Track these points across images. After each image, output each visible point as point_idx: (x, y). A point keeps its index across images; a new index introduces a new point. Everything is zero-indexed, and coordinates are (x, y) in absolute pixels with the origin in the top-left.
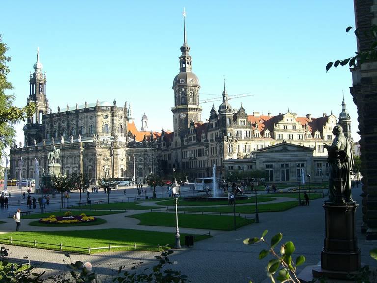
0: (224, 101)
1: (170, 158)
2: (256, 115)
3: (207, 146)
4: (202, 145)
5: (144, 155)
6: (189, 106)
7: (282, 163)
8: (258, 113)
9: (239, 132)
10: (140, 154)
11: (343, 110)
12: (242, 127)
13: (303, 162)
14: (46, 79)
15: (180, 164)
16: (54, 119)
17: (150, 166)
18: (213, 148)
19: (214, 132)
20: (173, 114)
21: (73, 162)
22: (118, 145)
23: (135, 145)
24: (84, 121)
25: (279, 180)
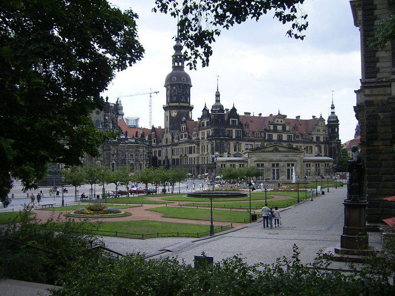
1: (160, 155)
2: (247, 115)
3: (198, 145)
4: (193, 142)
6: (181, 104)
11: (333, 113)
12: (234, 126)
15: (171, 160)
18: (204, 146)
19: (205, 131)
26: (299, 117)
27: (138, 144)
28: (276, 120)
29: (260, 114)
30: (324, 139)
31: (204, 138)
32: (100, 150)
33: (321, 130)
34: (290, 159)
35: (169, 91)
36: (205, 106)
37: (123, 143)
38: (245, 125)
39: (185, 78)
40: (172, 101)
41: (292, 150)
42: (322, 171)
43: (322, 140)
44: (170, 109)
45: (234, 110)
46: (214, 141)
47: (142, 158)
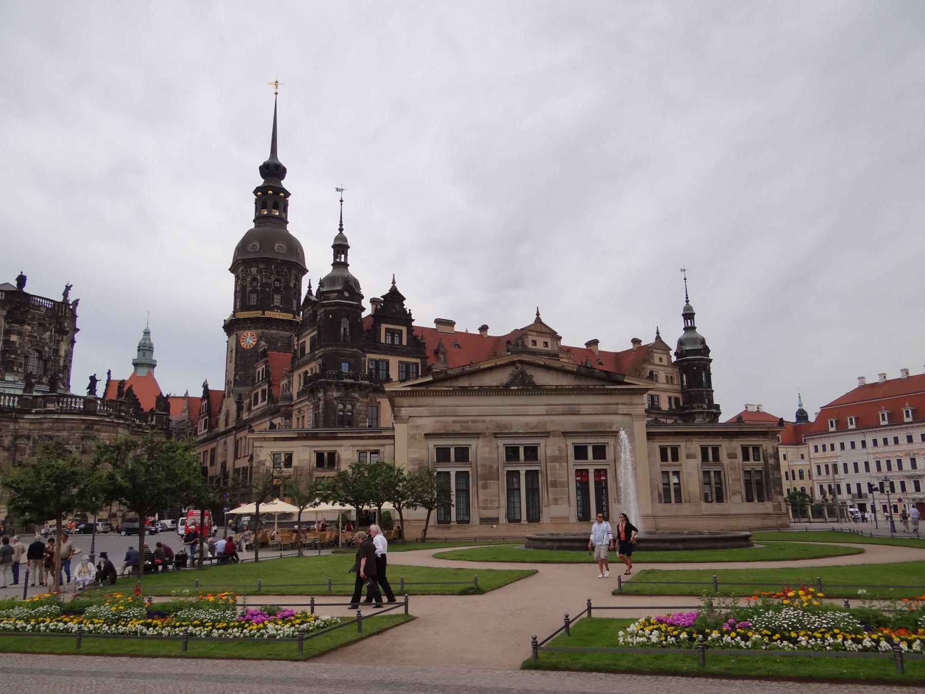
0: (336, 265)
2: (444, 329)
5: (83, 438)
6: (268, 314)
7: (510, 442)
8: (451, 324)
9: (382, 366)
10: (65, 434)
11: (690, 329)
12: (392, 350)
13: (600, 441)
23: (51, 407)
25: (495, 520)
26: (595, 342)
28: (530, 338)
29: (484, 328)
30: (670, 403)
33: (662, 377)
34: (583, 425)
37: (37, 413)
38: (436, 352)
41: (591, 383)
42: (734, 482)
43: (664, 406)
44: (239, 329)
45: (394, 297)
46: (321, 395)
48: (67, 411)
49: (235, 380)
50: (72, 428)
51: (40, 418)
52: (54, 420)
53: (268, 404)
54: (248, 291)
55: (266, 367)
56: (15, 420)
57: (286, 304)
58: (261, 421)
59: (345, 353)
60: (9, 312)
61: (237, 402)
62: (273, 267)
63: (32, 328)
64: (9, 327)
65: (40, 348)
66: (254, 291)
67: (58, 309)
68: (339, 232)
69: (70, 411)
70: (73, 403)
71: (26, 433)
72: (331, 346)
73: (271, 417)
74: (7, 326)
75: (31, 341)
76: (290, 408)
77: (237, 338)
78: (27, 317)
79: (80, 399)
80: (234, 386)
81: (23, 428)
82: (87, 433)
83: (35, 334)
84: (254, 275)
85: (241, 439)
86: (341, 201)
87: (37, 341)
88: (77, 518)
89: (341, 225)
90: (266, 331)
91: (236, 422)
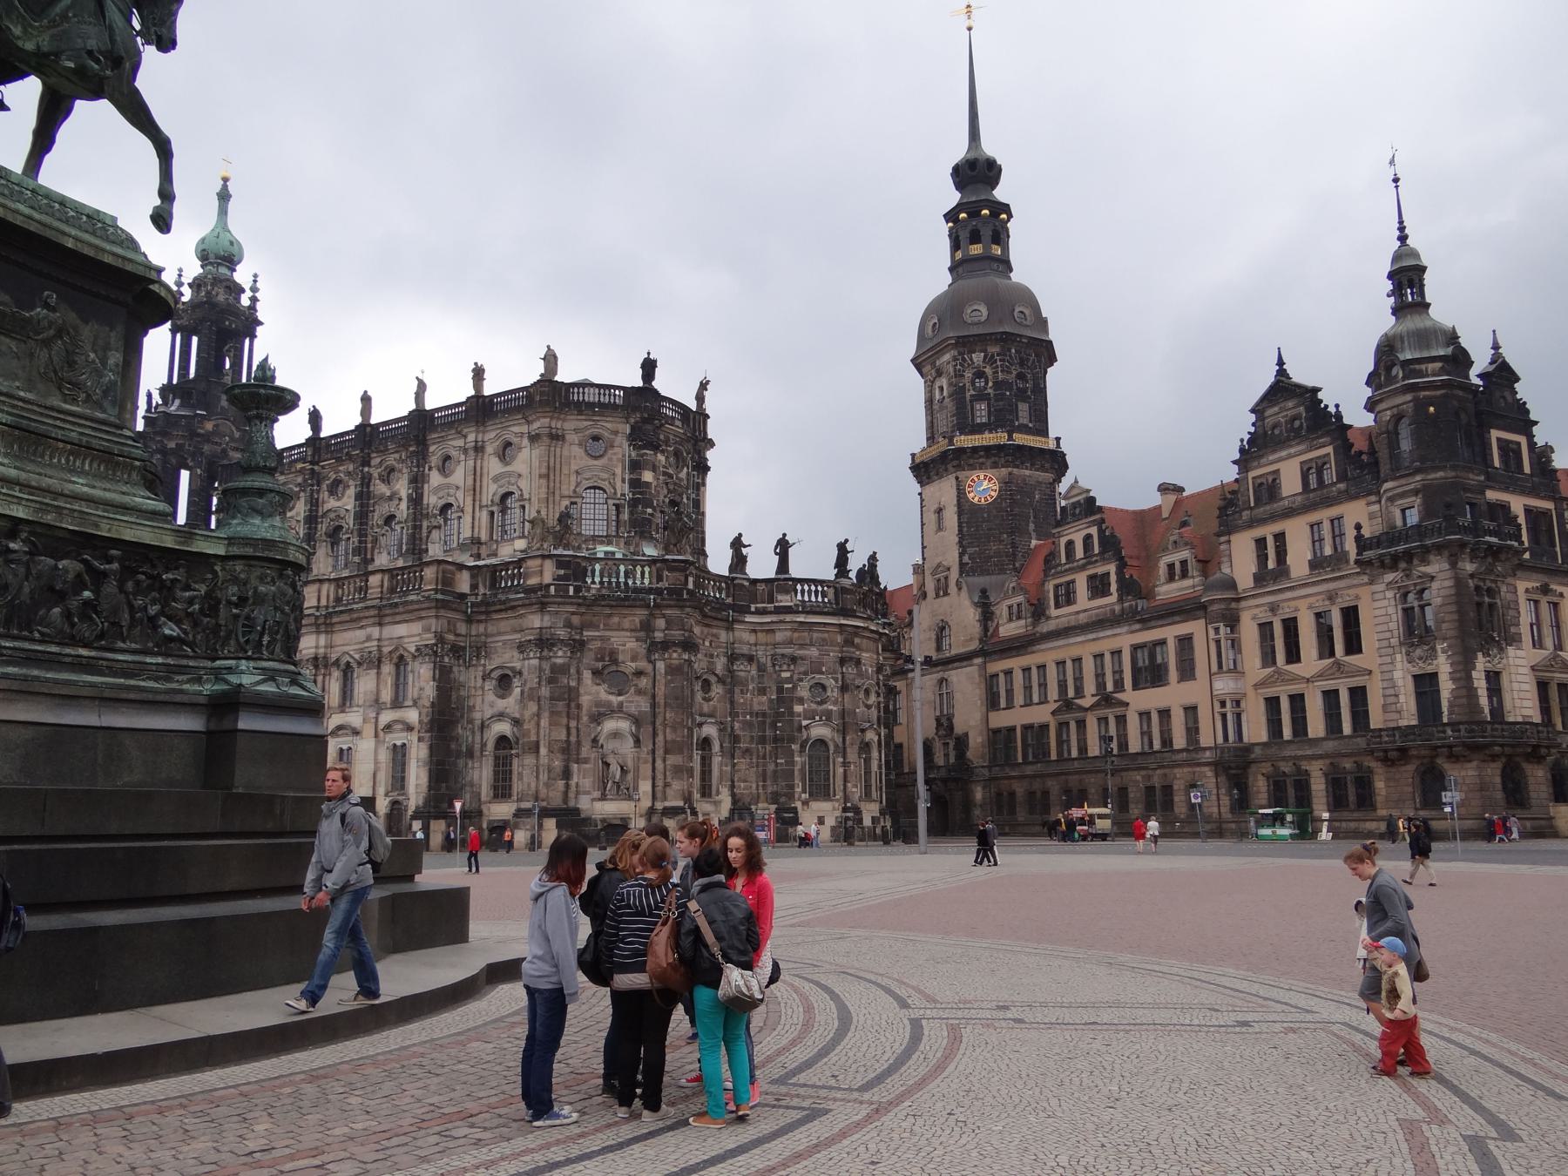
3: (1233, 621)
5: (842, 661)
6: (1021, 439)
10: (813, 652)
12: (1511, 478)
14: (260, 316)
15: (976, 740)
16: (283, 477)
17: (871, 736)
20: (918, 488)
21: (387, 695)
22: (691, 586)
23: (784, 600)
24: (459, 476)
27: (854, 616)
31: (1282, 570)
32: (632, 644)
35: (944, 382)
36: (1282, 372)
37: (760, 612)
39: (1027, 312)
40: (966, 425)
44: (959, 467)
46: (1437, 567)
47: (874, 713)
48: (814, 609)
49: (962, 565)
50: (824, 642)
51: (772, 622)
52: (795, 626)
53: (1121, 600)
54: (968, 398)
55: (1101, 532)
56: (730, 628)
57: (1039, 421)
58: (1093, 636)
59: (1469, 484)
60: (633, 428)
61: (976, 605)
62: (1013, 351)
63: (667, 458)
64: (638, 455)
65: (677, 499)
66: (981, 396)
67: (694, 424)
68: (1399, 243)
69: (818, 609)
70: (806, 594)
71: (745, 650)
72: (1443, 468)
73: (1137, 626)
74: (633, 454)
75: (667, 484)
76: (1233, 605)
77: (958, 485)
78: (658, 439)
79: (828, 587)
80: (961, 575)
81: (741, 642)
82: (847, 652)
83: (671, 471)
84: (979, 366)
85: (1009, 673)
86: (1396, 180)
87: (675, 484)
88: (850, 814)
89: (1402, 228)
90: (1015, 471)
91: (981, 641)
